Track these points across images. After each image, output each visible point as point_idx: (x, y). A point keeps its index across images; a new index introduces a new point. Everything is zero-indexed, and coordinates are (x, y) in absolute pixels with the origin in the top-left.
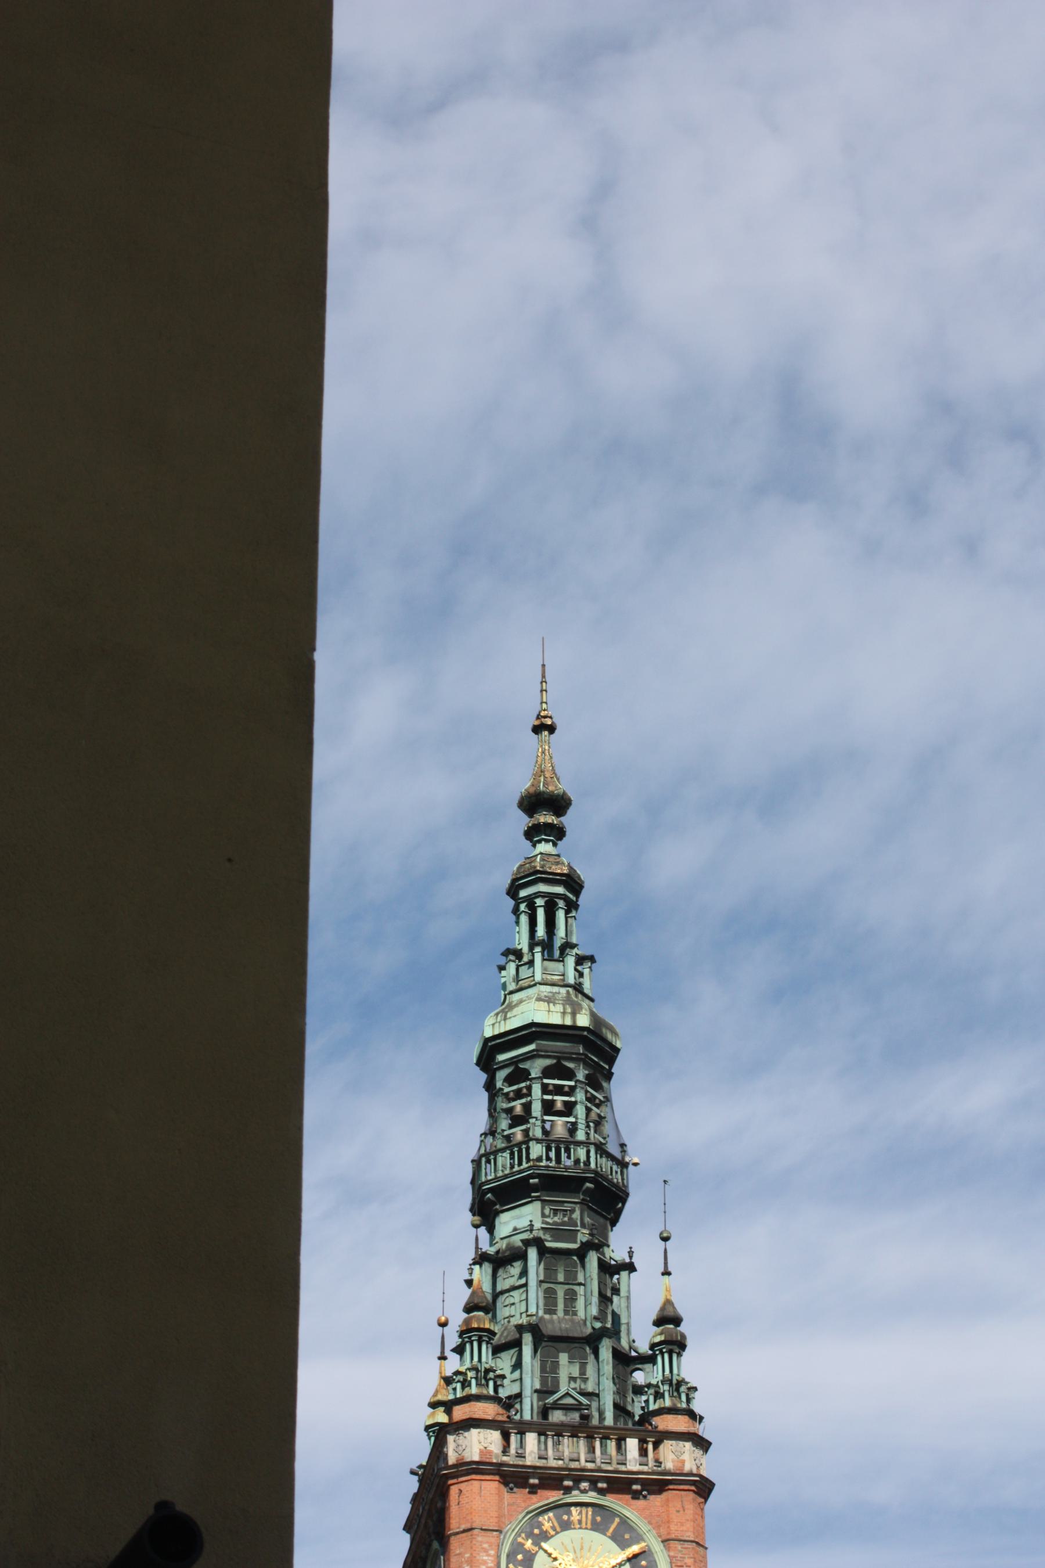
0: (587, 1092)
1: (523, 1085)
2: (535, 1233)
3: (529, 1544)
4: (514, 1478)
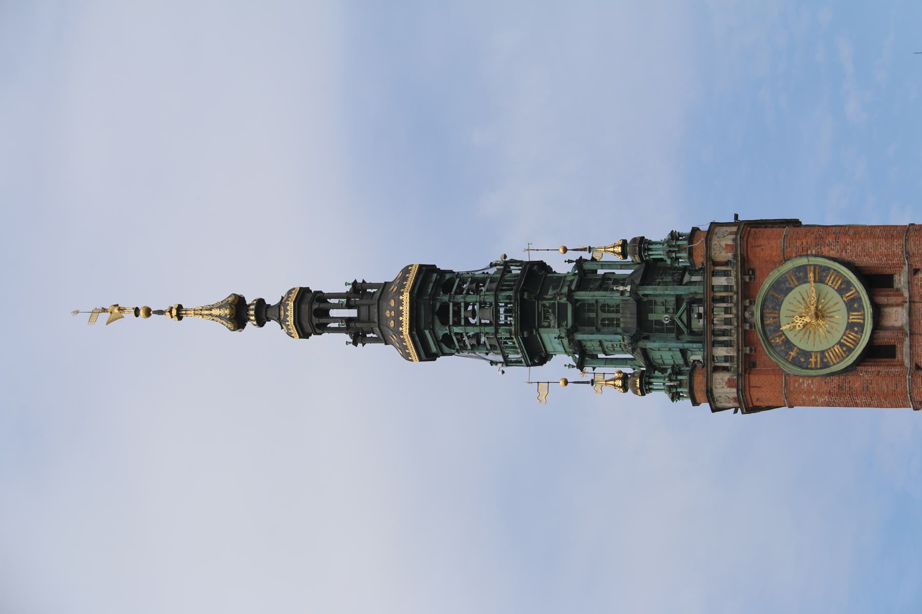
0: (456, 293)
1: (454, 338)
2: (563, 335)
3: (793, 354)
4: (748, 365)
